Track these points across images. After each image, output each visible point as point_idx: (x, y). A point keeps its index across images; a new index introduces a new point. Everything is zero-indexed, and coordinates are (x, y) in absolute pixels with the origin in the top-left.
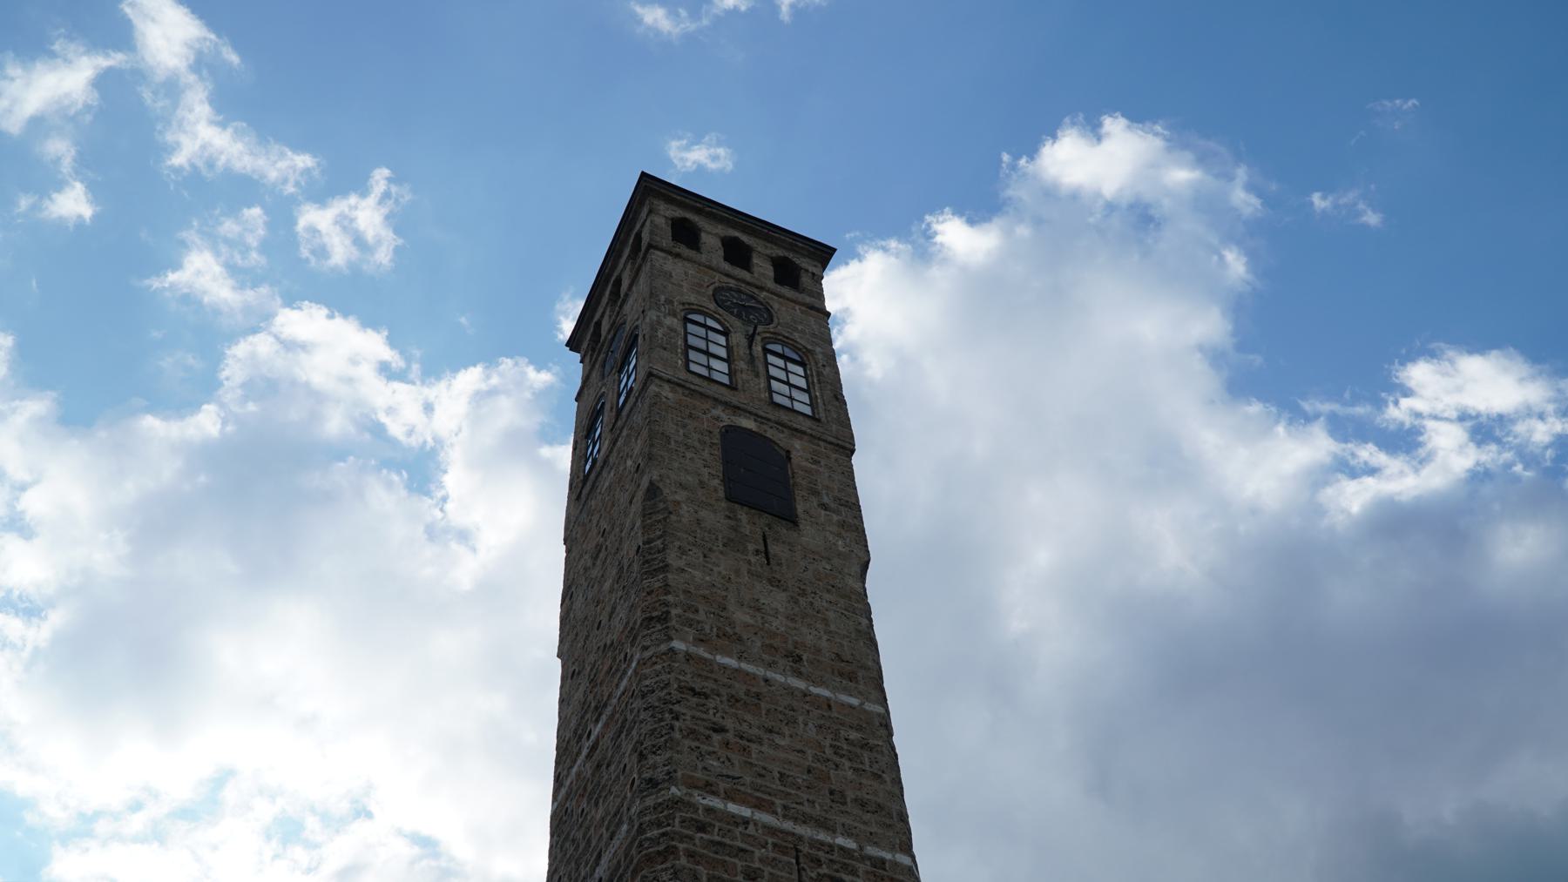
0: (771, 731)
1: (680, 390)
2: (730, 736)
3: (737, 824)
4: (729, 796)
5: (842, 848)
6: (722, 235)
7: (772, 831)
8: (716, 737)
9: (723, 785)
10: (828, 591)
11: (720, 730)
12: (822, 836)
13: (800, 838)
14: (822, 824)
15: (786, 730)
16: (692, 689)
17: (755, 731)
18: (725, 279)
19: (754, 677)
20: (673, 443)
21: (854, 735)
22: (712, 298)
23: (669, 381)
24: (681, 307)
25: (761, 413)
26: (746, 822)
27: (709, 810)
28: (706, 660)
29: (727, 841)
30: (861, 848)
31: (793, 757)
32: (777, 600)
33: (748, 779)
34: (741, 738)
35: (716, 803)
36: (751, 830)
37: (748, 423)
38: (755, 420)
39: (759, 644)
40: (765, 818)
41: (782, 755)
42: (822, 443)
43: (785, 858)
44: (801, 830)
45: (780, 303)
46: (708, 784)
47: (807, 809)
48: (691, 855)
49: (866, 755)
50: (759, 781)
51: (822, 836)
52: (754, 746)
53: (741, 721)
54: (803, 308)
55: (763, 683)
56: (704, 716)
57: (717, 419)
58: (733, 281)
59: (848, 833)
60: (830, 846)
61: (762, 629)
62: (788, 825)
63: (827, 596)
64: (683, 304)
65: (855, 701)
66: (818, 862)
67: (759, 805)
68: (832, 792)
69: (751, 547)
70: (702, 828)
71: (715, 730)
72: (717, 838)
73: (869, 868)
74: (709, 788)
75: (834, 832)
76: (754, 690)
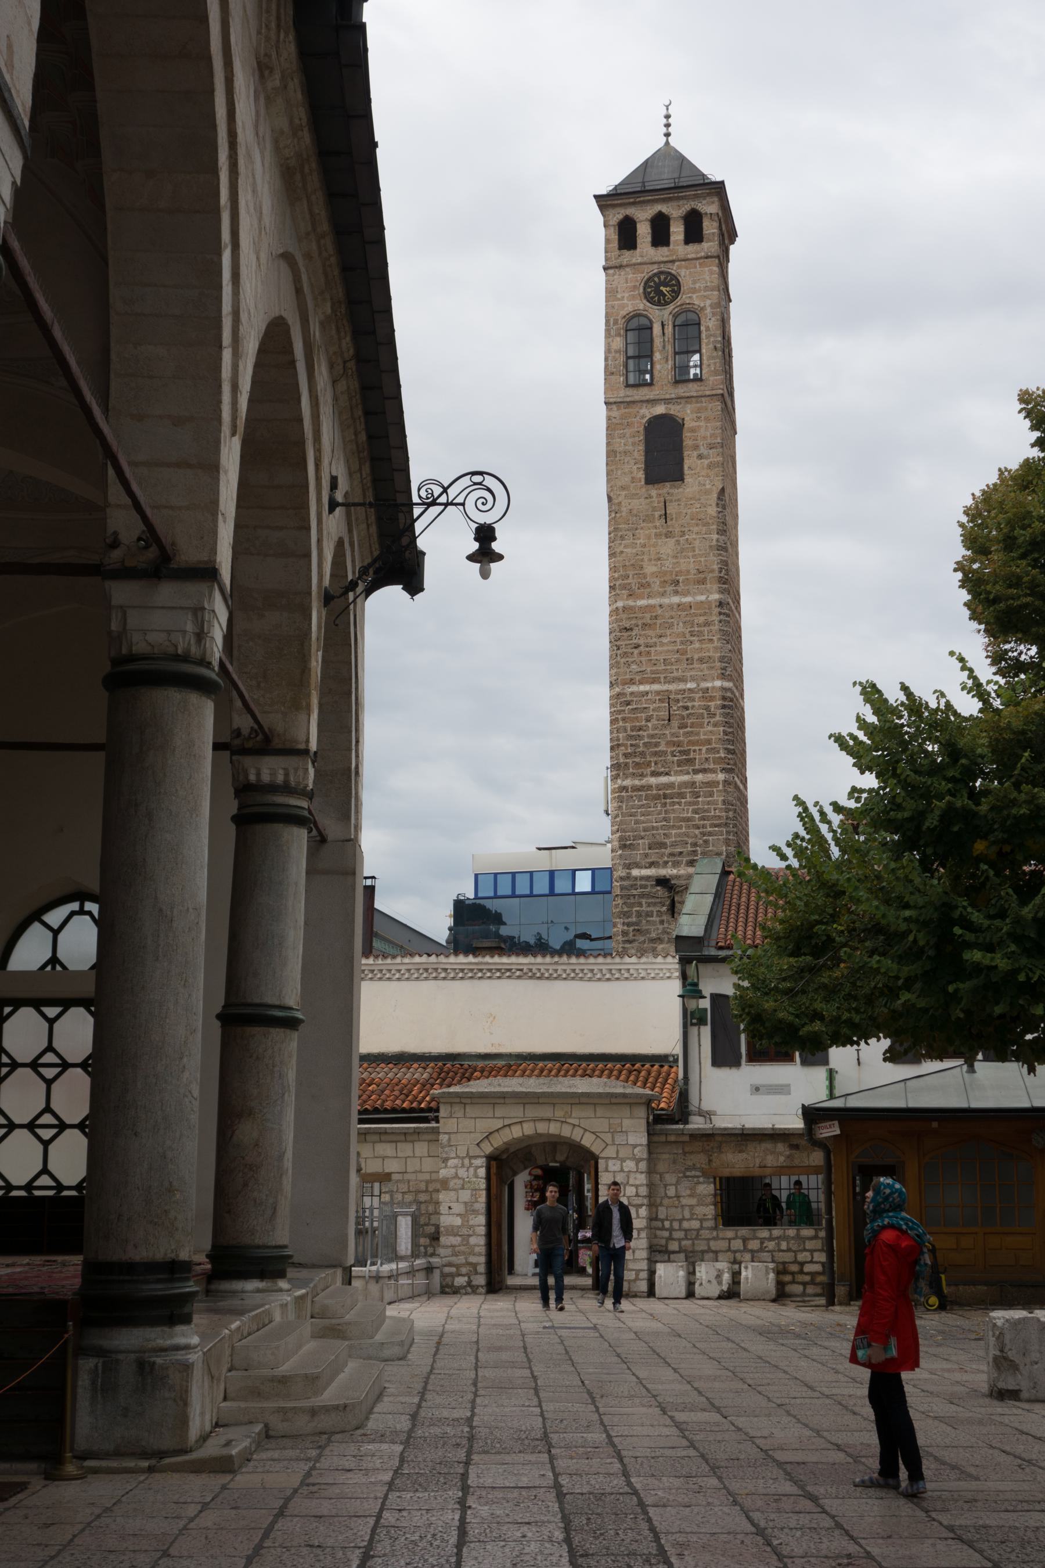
0: (661, 636)
1: (622, 406)
2: (642, 648)
3: (643, 696)
4: (641, 683)
5: (689, 689)
6: (649, 218)
7: (658, 693)
8: (636, 651)
9: (638, 678)
10: (697, 525)
11: (637, 647)
12: (682, 686)
13: (671, 692)
14: (682, 680)
15: (668, 632)
16: (626, 628)
17: (654, 640)
18: (651, 267)
19: (653, 607)
20: (618, 455)
21: (702, 619)
22: (643, 297)
23: (615, 403)
24: (624, 320)
25: (668, 396)
26: (647, 693)
27: (632, 693)
28: (632, 607)
29: (639, 706)
30: (698, 685)
31: (670, 648)
32: (668, 547)
33: (649, 669)
34: (647, 646)
35: (634, 688)
36: (649, 696)
37: (660, 410)
38: (665, 403)
39: (658, 583)
40: (656, 687)
41: (665, 648)
42: (703, 399)
43: (663, 705)
44: (672, 687)
45: (687, 268)
46: (632, 679)
47: (675, 674)
48: (624, 719)
49: (706, 629)
50: (654, 668)
51: (682, 686)
52: (652, 649)
53: (647, 636)
54: (702, 261)
55: (658, 608)
56: (631, 642)
57: (643, 417)
58: (656, 266)
59: (693, 679)
60: (684, 690)
61: (659, 572)
62: (666, 687)
63: (696, 529)
64: (625, 317)
65: (703, 598)
66: (678, 701)
67: (654, 681)
68: (687, 660)
69: (657, 514)
70: (628, 703)
71: (636, 648)
72: (635, 707)
73: (701, 695)
74: (632, 682)
75: (686, 682)
76: (654, 614)
